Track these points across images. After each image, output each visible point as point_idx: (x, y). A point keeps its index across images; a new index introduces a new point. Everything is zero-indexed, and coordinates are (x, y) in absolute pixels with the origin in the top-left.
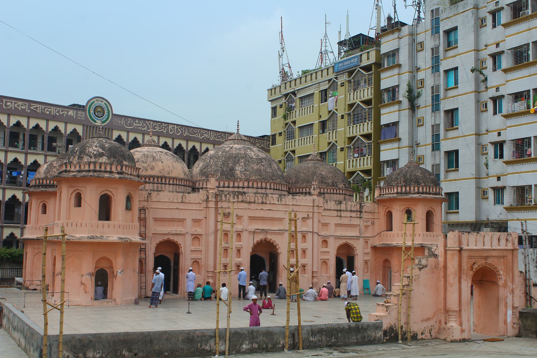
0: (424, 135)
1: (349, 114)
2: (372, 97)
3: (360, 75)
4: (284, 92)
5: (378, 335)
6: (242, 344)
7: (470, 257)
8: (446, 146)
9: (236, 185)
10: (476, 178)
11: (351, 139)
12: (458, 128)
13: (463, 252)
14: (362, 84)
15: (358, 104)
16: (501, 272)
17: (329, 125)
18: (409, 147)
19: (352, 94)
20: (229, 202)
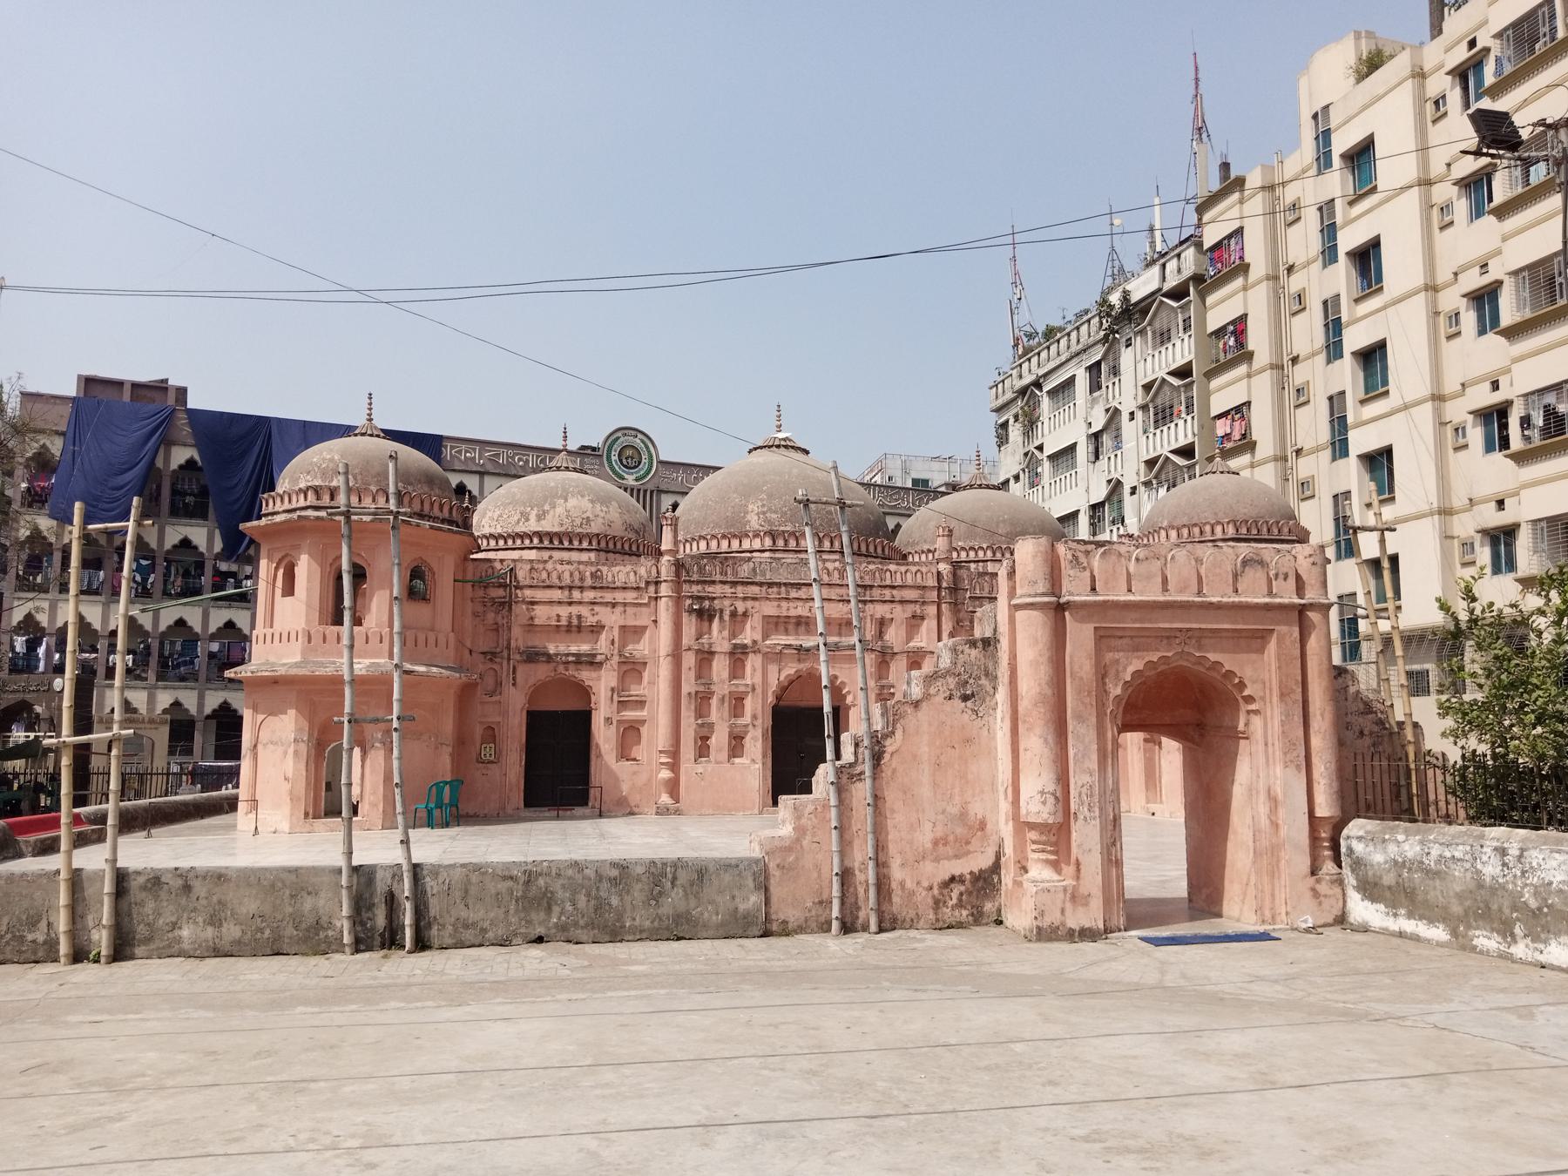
0: (1313, 426)
1: (1144, 408)
2: (1192, 357)
3: (1163, 314)
4: (1019, 384)
5: (742, 907)
6: (174, 926)
8: (1362, 441)
9: (746, 545)
10: (1440, 513)
11: (1151, 463)
12: (1387, 392)
14: (1173, 332)
15: (1164, 380)
17: (1106, 440)
18: (1276, 459)
19: (1149, 359)
20: (713, 582)
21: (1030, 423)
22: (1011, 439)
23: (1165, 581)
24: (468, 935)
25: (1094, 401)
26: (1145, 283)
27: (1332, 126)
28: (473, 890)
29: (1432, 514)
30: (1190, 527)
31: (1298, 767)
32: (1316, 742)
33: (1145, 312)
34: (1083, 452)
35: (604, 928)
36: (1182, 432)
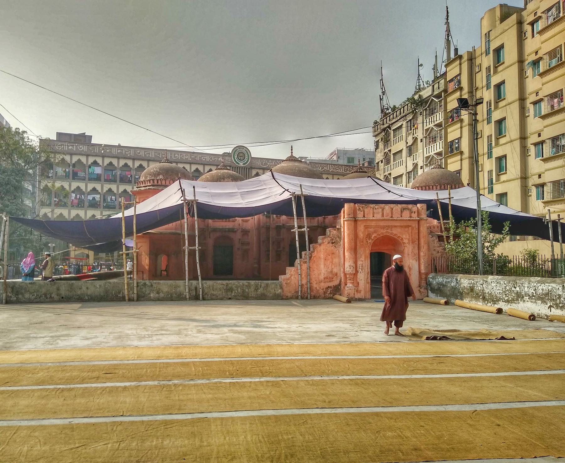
1: (426, 137)
3: (433, 103)
4: (382, 127)
7: (366, 227)
13: (359, 223)
16: (406, 241)
21: (386, 141)
22: (380, 147)
23: (383, 214)
24: (214, 297)
25: (409, 134)
26: (427, 92)
27: (491, 39)
28: (215, 287)
29: (517, 179)
30: (425, 187)
31: (416, 260)
32: (422, 254)
33: (427, 102)
34: (404, 153)
35: (244, 296)
36: (439, 147)
